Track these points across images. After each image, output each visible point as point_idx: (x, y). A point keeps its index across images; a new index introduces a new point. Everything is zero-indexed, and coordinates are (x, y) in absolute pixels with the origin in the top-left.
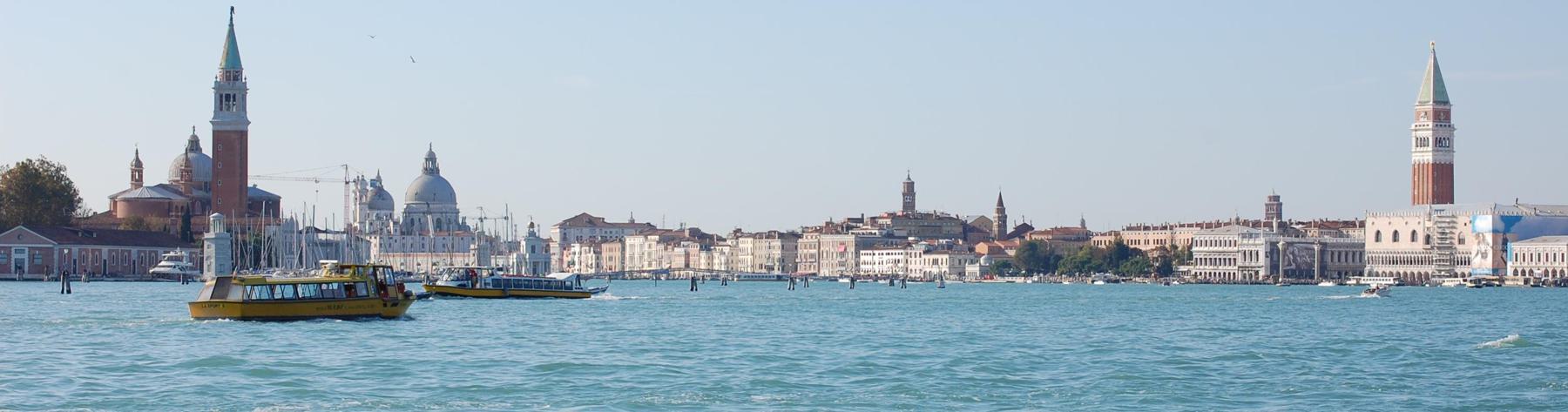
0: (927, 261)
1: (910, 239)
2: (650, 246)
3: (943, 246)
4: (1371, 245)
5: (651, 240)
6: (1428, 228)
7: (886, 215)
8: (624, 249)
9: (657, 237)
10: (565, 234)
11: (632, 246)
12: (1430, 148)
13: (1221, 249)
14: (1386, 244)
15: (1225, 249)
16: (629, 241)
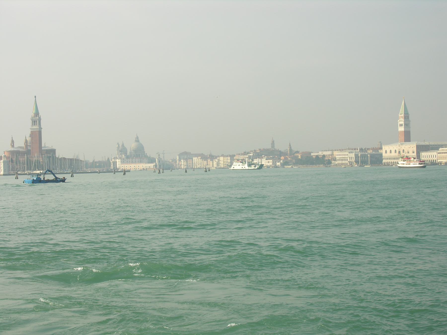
0: (267, 162)
1: (263, 156)
2: (199, 159)
3: (271, 158)
4: (384, 154)
5: (199, 158)
6: (399, 149)
7: (258, 150)
8: (193, 161)
9: (200, 157)
10: (180, 157)
11: (194, 160)
12: (403, 127)
13: (343, 156)
14: (388, 154)
15: (345, 156)
16: (194, 159)
